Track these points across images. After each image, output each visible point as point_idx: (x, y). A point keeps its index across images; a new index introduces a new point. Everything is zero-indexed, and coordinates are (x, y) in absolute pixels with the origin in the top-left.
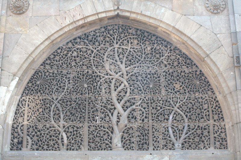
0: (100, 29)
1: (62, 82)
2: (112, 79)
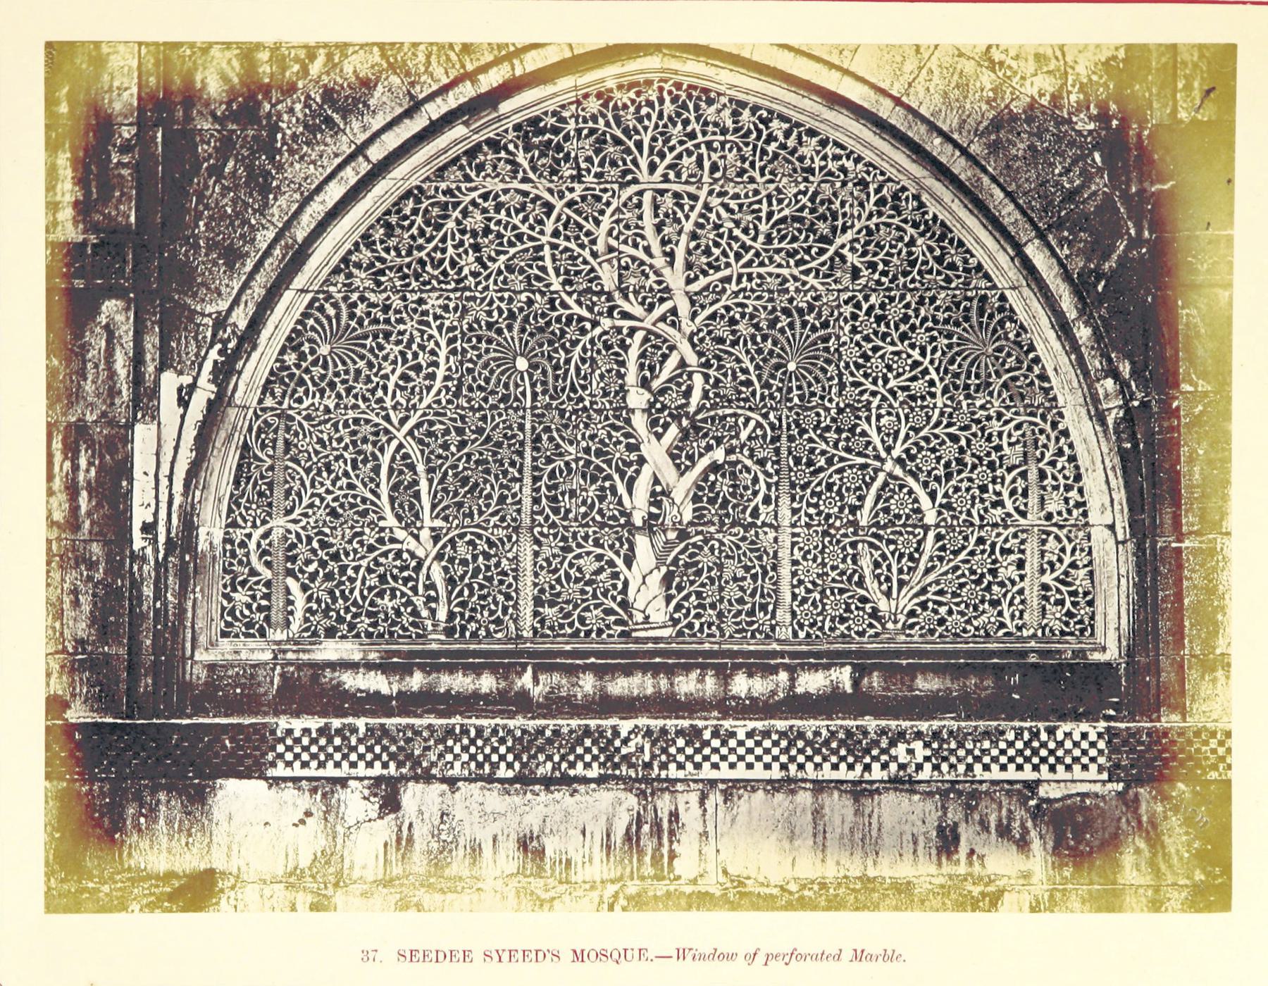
0: (578, 102)
1: (422, 347)
2: (633, 331)
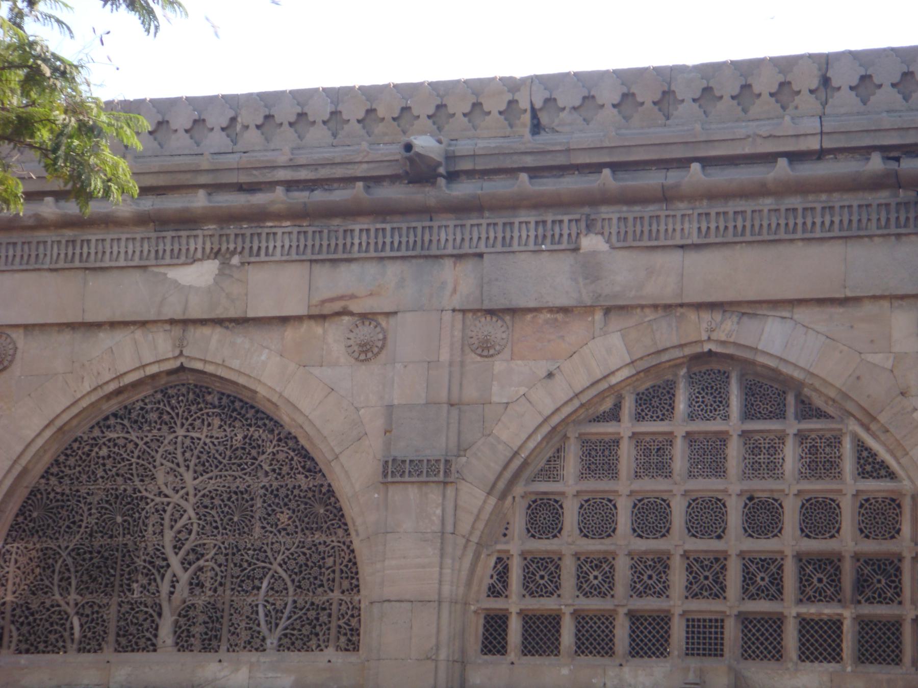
0: (153, 395)
2: (168, 504)
